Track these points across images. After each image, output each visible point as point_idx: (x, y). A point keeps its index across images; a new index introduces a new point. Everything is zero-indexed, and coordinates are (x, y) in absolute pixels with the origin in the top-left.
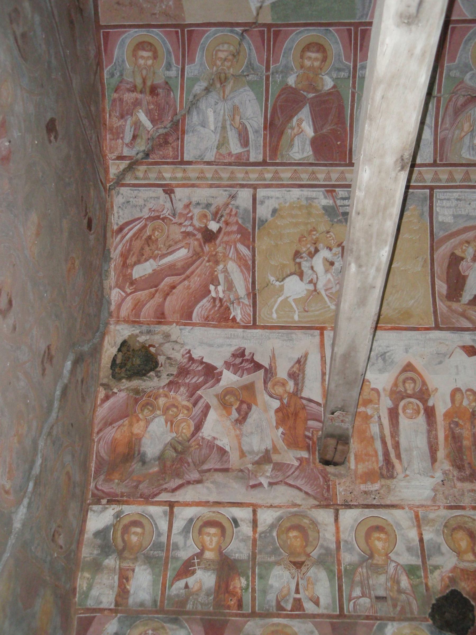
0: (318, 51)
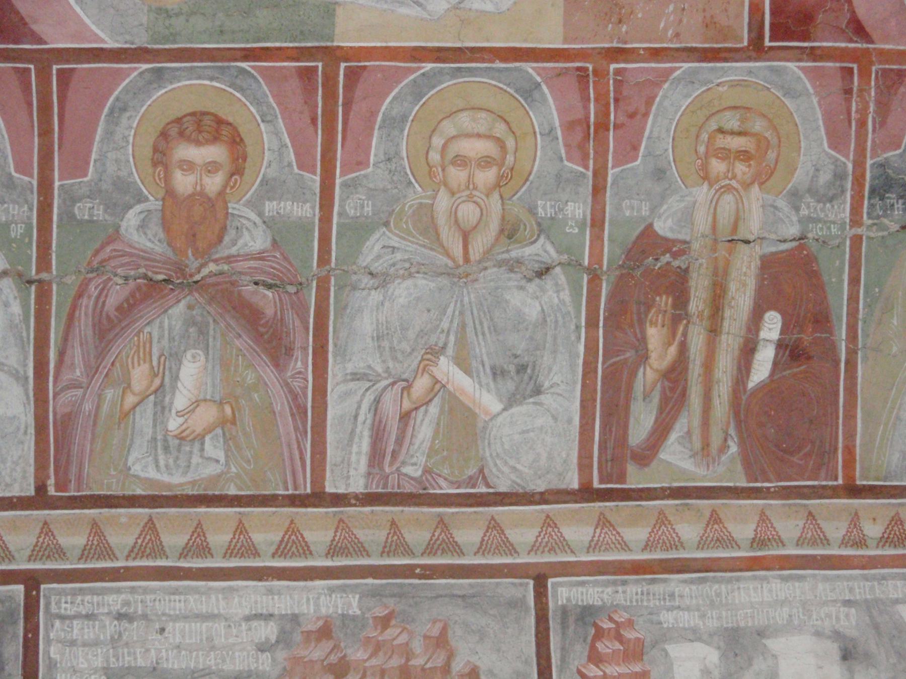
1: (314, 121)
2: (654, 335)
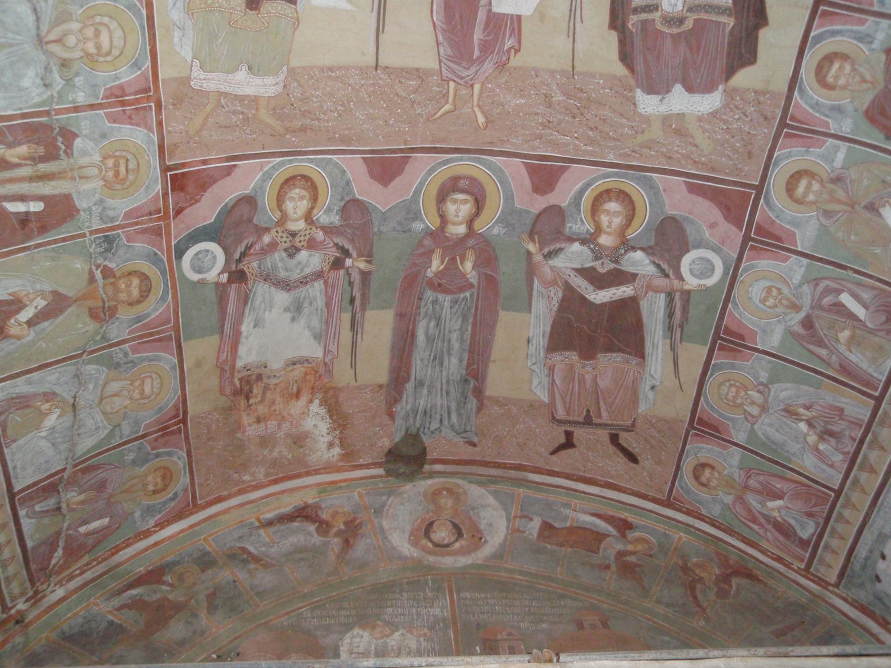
2: (23, 149)
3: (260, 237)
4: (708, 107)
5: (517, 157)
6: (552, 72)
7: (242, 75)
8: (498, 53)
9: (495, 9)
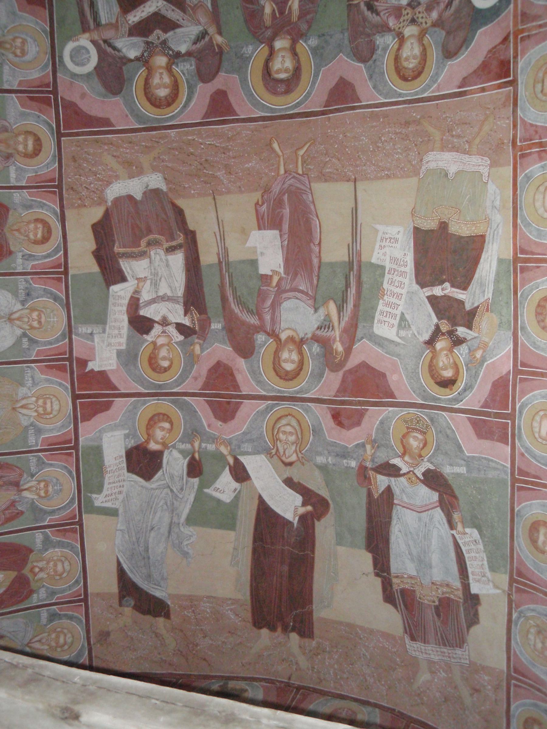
0: (538, 531)
1: (538, 267)
3: (440, 16)
4: (114, 188)
5: (244, 119)
6: (229, 192)
7: (453, 169)
8: (270, 200)
9: (276, 232)
